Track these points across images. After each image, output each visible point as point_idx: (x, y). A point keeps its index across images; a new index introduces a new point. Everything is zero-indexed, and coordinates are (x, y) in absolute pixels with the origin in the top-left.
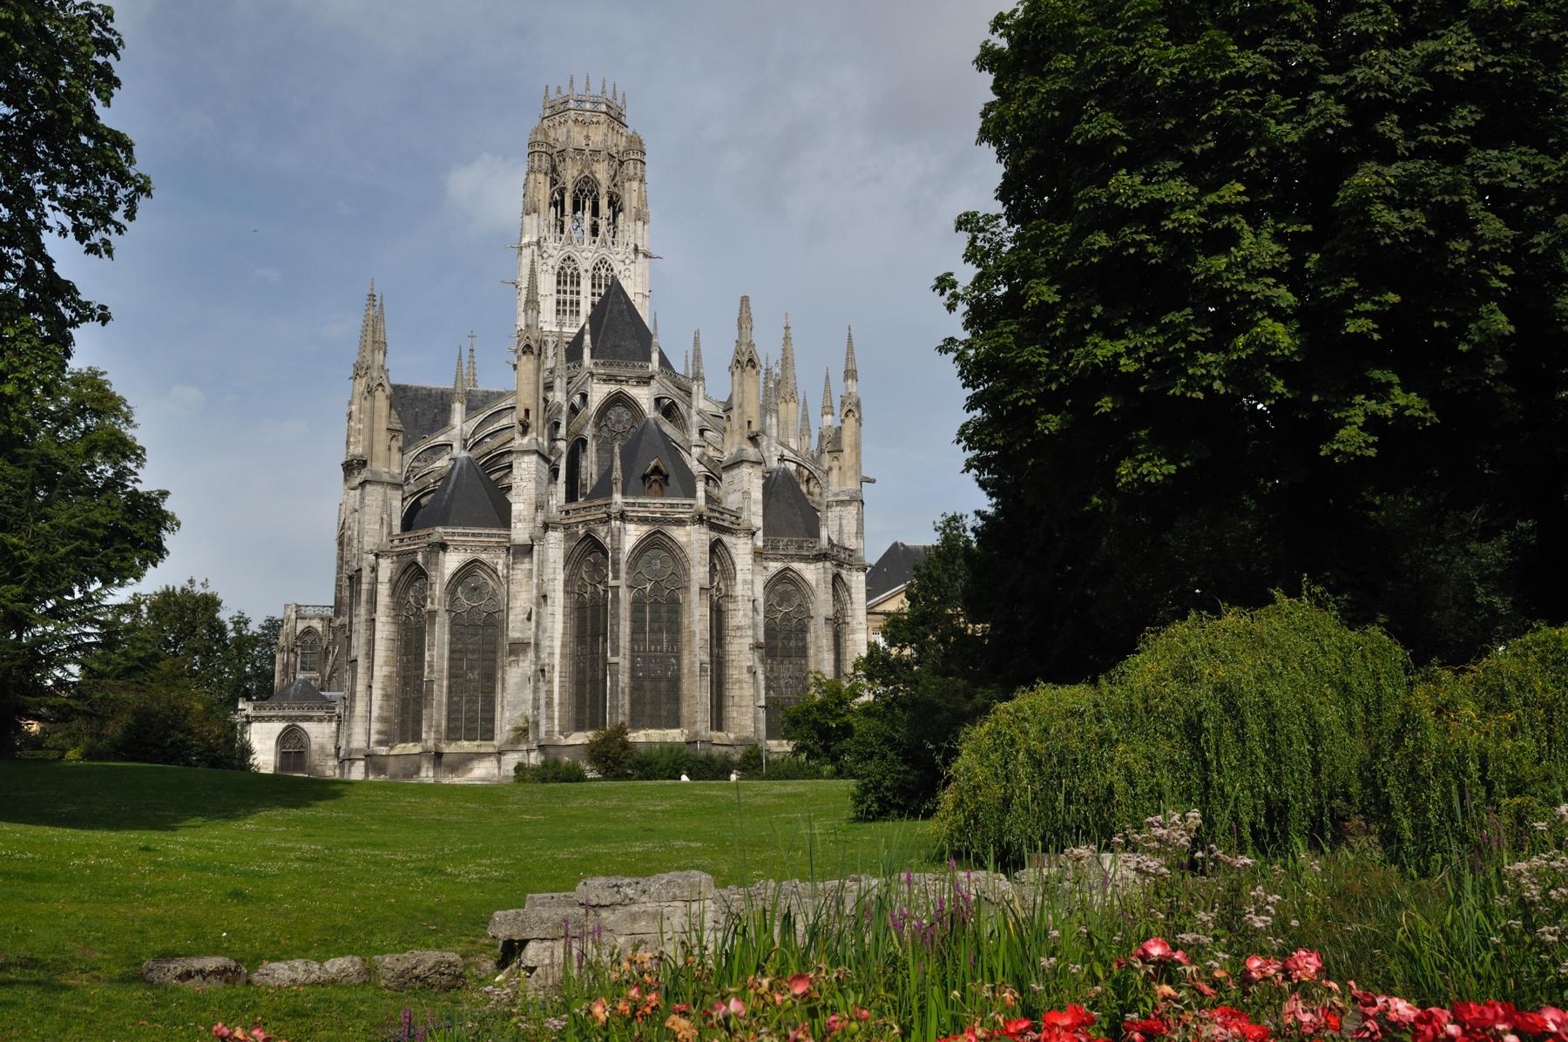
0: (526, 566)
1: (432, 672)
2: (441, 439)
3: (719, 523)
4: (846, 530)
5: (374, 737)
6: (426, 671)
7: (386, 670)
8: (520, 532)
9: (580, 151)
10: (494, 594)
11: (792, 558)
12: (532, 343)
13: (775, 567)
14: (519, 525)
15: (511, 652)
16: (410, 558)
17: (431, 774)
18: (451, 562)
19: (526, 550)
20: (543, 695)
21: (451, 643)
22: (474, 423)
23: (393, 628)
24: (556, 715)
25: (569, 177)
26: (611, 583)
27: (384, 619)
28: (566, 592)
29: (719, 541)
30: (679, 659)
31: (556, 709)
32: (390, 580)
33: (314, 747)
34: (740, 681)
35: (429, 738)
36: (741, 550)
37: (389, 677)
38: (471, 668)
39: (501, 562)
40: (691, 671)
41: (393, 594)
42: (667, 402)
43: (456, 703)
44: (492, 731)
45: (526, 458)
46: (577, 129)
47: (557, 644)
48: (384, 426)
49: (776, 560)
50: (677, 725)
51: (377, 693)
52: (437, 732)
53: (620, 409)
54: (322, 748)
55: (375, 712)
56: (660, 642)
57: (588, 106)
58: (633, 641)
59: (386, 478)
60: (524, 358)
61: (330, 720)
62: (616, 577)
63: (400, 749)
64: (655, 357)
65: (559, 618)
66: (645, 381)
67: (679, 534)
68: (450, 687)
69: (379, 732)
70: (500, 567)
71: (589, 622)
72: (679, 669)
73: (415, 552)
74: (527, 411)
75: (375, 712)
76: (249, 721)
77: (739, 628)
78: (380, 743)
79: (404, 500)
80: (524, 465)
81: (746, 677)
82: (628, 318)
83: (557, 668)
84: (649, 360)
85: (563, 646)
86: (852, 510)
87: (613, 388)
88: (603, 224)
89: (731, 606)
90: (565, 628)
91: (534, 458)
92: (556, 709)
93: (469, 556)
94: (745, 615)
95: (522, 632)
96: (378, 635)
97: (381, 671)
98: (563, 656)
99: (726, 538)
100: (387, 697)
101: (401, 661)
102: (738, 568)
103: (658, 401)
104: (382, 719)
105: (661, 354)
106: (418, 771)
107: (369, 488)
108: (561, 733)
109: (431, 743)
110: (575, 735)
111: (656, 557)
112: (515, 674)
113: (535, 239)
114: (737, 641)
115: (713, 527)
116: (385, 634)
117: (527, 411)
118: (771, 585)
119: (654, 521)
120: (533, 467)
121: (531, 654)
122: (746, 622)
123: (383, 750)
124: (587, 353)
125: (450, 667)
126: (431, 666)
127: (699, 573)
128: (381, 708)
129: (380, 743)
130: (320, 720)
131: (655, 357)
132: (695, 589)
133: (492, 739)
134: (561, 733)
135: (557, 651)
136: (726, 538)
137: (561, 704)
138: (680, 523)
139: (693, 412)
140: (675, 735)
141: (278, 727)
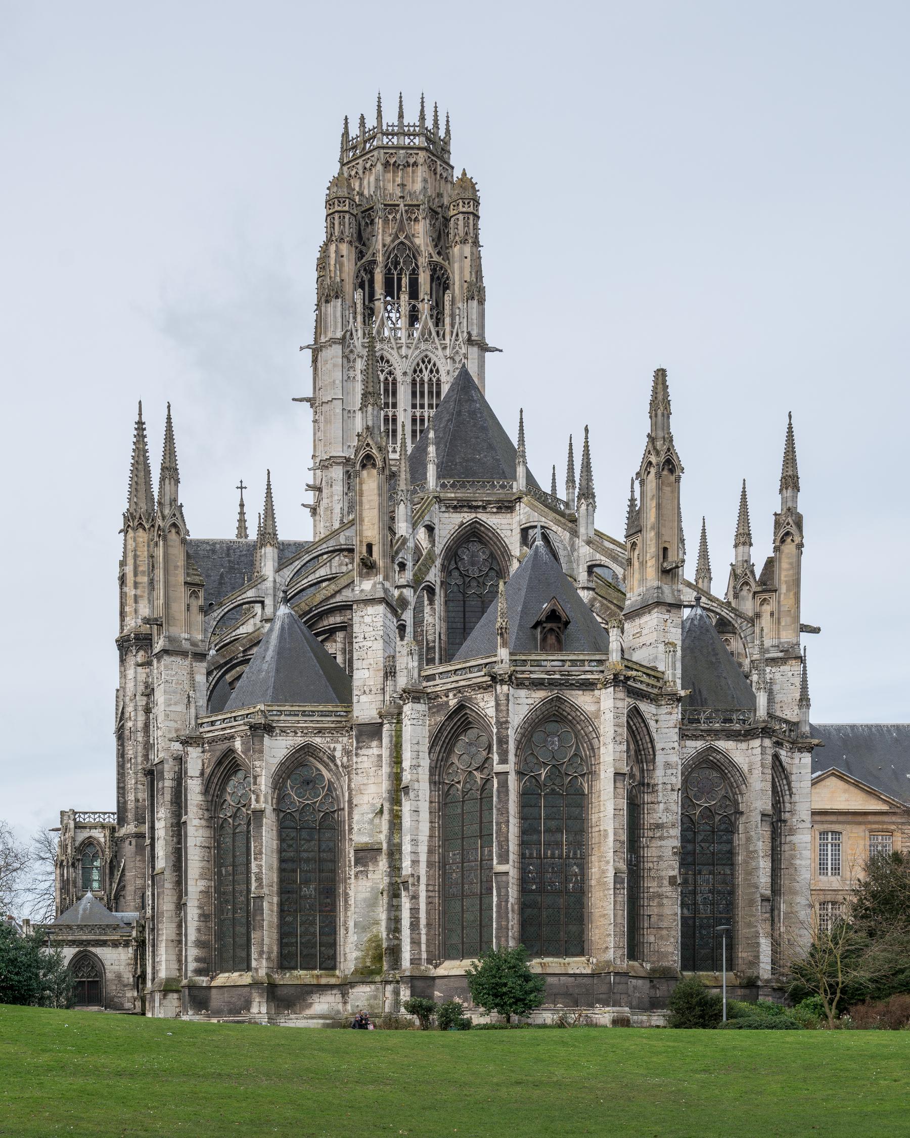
1: (260, 886)
2: (251, 594)
5: (192, 965)
6: (254, 885)
7: (202, 885)
8: (366, 708)
10: (331, 787)
11: (717, 734)
14: (364, 698)
16: (224, 746)
17: (264, 1010)
18: (278, 749)
20: (406, 915)
21: (281, 851)
22: (288, 573)
23: (207, 833)
24: (424, 938)
26: (498, 768)
27: (196, 822)
28: (432, 782)
31: (423, 931)
32: (202, 774)
33: (109, 975)
34: (660, 896)
35: (261, 967)
37: (205, 893)
38: (306, 882)
39: (339, 747)
41: (206, 792)
44: (334, 957)
45: (371, 610)
47: (423, 849)
48: (181, 579)
49: (695, 738)
51: (193, 913)
52: (269, 959)
53: (475, 547)
54: (119, 977)
55: (192, 935)
56: (559, 844)
58: (523, 844)
61: (127, 944)
63: (222, 979)
65: (425, 816)
66: (507, 506)
68: (281, 904)
69: (198, 960)
70: (338, 754)
71: (461, 818)
73: (232, 737)
75: (192, 935)
77: (659, 826)
78: (199, 972)
80: (367, 619)
83: (423, 880)
84: (515, 478)
85: (430, 852)
86: (791, 670)
87: (467, 517)
88: (424, 308)
90: (432, 829)
91: (381, 609)
93: (299, 740)
94: (667, 810)
95: (371, 836)
96: (191, 842)
97: (195, 885)
98: (430, 864)
99: (646, 708)
100: (204, 917)
103: (525, 532)
104: (200, 944)
106: (247, 1005)
108: (429, 961)
109: (262, 973)
110: (447, 964)
116: (199, 841)
121: (383, 863)
123: (203, 981)
124: (431, 472)
125: (281, 881)
126: (259, 879)
127: (610, 754)
128: (199, 930)
129: (199, 972)
130: (115, 944)
134: (429, 961)
135: (423, 858)
136: (646, 708)
137: (428, 925)
140: (577, 965)
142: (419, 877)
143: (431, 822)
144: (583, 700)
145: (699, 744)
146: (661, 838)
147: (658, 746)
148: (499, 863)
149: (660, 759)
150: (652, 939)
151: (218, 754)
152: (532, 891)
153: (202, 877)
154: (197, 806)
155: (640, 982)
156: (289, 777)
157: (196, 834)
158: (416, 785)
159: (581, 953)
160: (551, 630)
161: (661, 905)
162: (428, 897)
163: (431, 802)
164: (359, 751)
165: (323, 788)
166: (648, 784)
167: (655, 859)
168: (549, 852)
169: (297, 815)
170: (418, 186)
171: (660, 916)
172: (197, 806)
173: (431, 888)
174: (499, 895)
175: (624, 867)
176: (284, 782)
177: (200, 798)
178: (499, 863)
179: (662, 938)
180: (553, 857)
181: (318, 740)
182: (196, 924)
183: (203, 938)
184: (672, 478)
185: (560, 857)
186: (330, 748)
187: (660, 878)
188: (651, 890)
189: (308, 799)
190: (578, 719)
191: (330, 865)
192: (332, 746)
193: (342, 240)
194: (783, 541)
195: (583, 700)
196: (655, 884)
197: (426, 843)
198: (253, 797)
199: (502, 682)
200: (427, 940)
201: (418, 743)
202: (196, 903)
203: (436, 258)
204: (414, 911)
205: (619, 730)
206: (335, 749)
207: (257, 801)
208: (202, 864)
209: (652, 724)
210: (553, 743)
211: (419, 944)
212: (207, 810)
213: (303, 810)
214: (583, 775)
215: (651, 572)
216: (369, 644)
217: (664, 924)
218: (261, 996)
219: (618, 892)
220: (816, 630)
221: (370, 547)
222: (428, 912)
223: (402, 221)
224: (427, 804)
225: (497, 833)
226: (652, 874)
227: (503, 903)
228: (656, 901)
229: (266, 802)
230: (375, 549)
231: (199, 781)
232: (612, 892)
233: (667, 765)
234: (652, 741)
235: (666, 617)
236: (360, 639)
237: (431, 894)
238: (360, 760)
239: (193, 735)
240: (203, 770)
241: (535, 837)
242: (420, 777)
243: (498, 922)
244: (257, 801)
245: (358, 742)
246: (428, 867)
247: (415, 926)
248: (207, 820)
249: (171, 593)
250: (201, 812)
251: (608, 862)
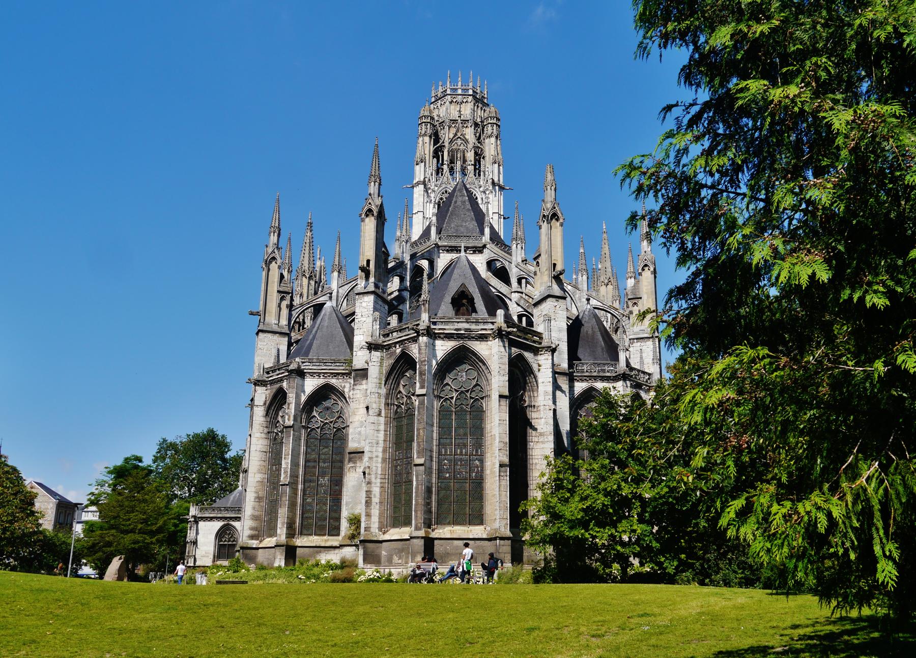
0: (364, 387)
3: (522, 338)
4: (646, 361)
7: (259, 477)
9: (455, 121)
12: (373, 208)
15: (350, 460)
16: (278, 386)
19: (363, 374)
23: (266, 442)
25: (447, 139)
27: (258, 435)
29: (520, 357)
30: (482, 461)
32: (265, 404)
36: (543, 367)
38: (323, 475)
39: (347, 385)
40: (492, 472)
42: (498, 265)
43: (309, 504)
46: (453, 106)
48: (276, 290)
50: (481, 523)
56: (465, 446)
57: (460, 92)
59: (275, 328)
60: (367, 220)
62: (422, 387)
64: (487, 231)
66: (479, 250)
67: (480, 348)
69: (252, 529)
70: (346, 390)
72: (482, 470)
74: (368, 261)
76: (197, 520)
78: (252, 537)
79: (290, 344)
80: (364, 304)
82: (469, 207)
89: (534, 415)
90: (386, 435)
100: (259, 499)
101: (272, 468)
102: (540, 381)
104: (255, 518)
105: (492, 228)
107: (260, 334)
110: (393, 531)
111: (462, 370)
112: (352, 478)
113: (422, 179)
114: (540, 446)
115: (513, 343)
116: (259, 447)
117: (368, 261)
119: (459, 337)
120: (371, 305)
122: (400, 334)
128: (254, 508)
129: (252, 537)
131: (487, 231)
132: (495, 396)
133: (338, 535)
138: (483, 338)
139: (513, 266)
141: (218, 525)
148: (418, 457)
151: (274, 390)
152: (446, 478)
153: (260, 472)
174: (417, 480)
177: (263, 419)
178: (418, 457)
180: (461, 454)
182: (252, 503)
183: (256, 513)
191: (339, 464)
198: (287, 417)
202: (254, 490)
214: (482, 398)
216: (364, 319)
218: (281, 554)
231: (263, 408)
239: (260, 379)
241: (448, 441)
243: (416, 500)
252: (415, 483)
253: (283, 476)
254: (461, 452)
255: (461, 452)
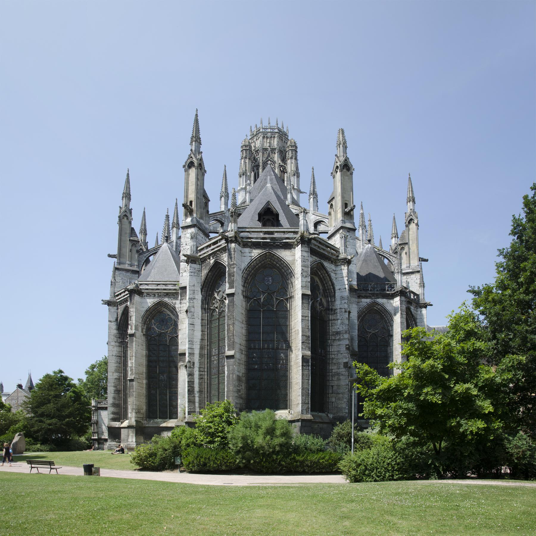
7: (116, 375)
13: (366, 301)
17: (134, 440)
24: (197, 399)
31: (197, 395)
34: (338, 374)
49: (366, 297)
70: (177, 306)
77: (338, 333)
81: (343, 370)
83: (197, 365)
90: (203, 335)
92: (197, 395)
98: (201, 355)
118: (362, 316)
123: (117, 424)
135: (197, 352)
137: (200, 391)
142: (194, 363)
143: (202, 331)
144: (285, 255)
145: (368, 301)
146: (339, 340)
147: (337, 288)
148: (228, 350)
149: (338, 294)
150: (334, 400)
152: (255, 369)
154: (114, 335)
155: (325, 426)
156: (153, 318)
157: (113, 350)
158: (192, 309)
159: (286, 408)
160: (268, 220)
161: (339, 380)
162: (200, 375)
163: (202, 320)
164: (182, 301)
165: (171, 324)
166: (332, 309)
167: (336, 353)
168: (266, 345)
169: (157, 338)
170: (276, 143)
171: (338, 386)
172: (114, 335)
173: (202, 369)
174: (228, 371)
175: (309, 353)
176: (150, 321)
178: (228, 350)
179: (339, 399)
181: (166, 300)
184: (349, 173)
185: (273, 349)
186: (172, 303)
187: (339, 364)
188: (333, 371)
189: (163, 330)
190: (282, 266)
192: (174, 302)
193: (246, 158)
194: (409, 223)
195: (285, 255)
196: (336, 367)
197: (199, 343)
199: (232, 242)
200: (200, 401)
201: (194, 286)
203: (282, 164)
204: (191, 383)
205: (305, 269)
206: (175, 303)
207: (131, 329)
208: (116, 365)
209: (333, 275)
210: (268, 281)
211: (194, 402)
212: (120, 338)
213: (160, 335)
215: (340, 216)
217: (341, 391)
219: (305, 368)
220: (426, 260)
221: (191, 202)
222: (200, 384)
223: (269, 153)
224: (200, 321)
225: (227, 331)
226: (334, 361)
227: (231, 375)
228: (336, 377)
229: (136, 329)
230: (193, 203)
232: (301, 368)
233: (342, 298)
234: (333, 284)
235: (348, 234)
236: (184, 245)
237: (202, 373)
238: (182, 306)
240: (117, 318)
242: (195, 305)
244: (131, 329)
245: (181, 297)
246: (200, 357)
247: (191, 391)
248: (120, 343)
249: (122, 244)
250: (116, 339)
251: (299, 350)
252: (226, 373)
253: (129, 373)
254: (268, 346)
255: (268, 346)
